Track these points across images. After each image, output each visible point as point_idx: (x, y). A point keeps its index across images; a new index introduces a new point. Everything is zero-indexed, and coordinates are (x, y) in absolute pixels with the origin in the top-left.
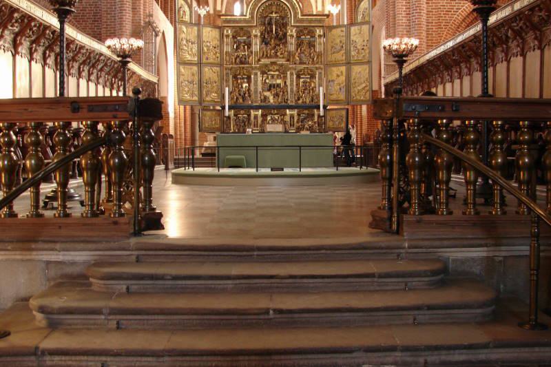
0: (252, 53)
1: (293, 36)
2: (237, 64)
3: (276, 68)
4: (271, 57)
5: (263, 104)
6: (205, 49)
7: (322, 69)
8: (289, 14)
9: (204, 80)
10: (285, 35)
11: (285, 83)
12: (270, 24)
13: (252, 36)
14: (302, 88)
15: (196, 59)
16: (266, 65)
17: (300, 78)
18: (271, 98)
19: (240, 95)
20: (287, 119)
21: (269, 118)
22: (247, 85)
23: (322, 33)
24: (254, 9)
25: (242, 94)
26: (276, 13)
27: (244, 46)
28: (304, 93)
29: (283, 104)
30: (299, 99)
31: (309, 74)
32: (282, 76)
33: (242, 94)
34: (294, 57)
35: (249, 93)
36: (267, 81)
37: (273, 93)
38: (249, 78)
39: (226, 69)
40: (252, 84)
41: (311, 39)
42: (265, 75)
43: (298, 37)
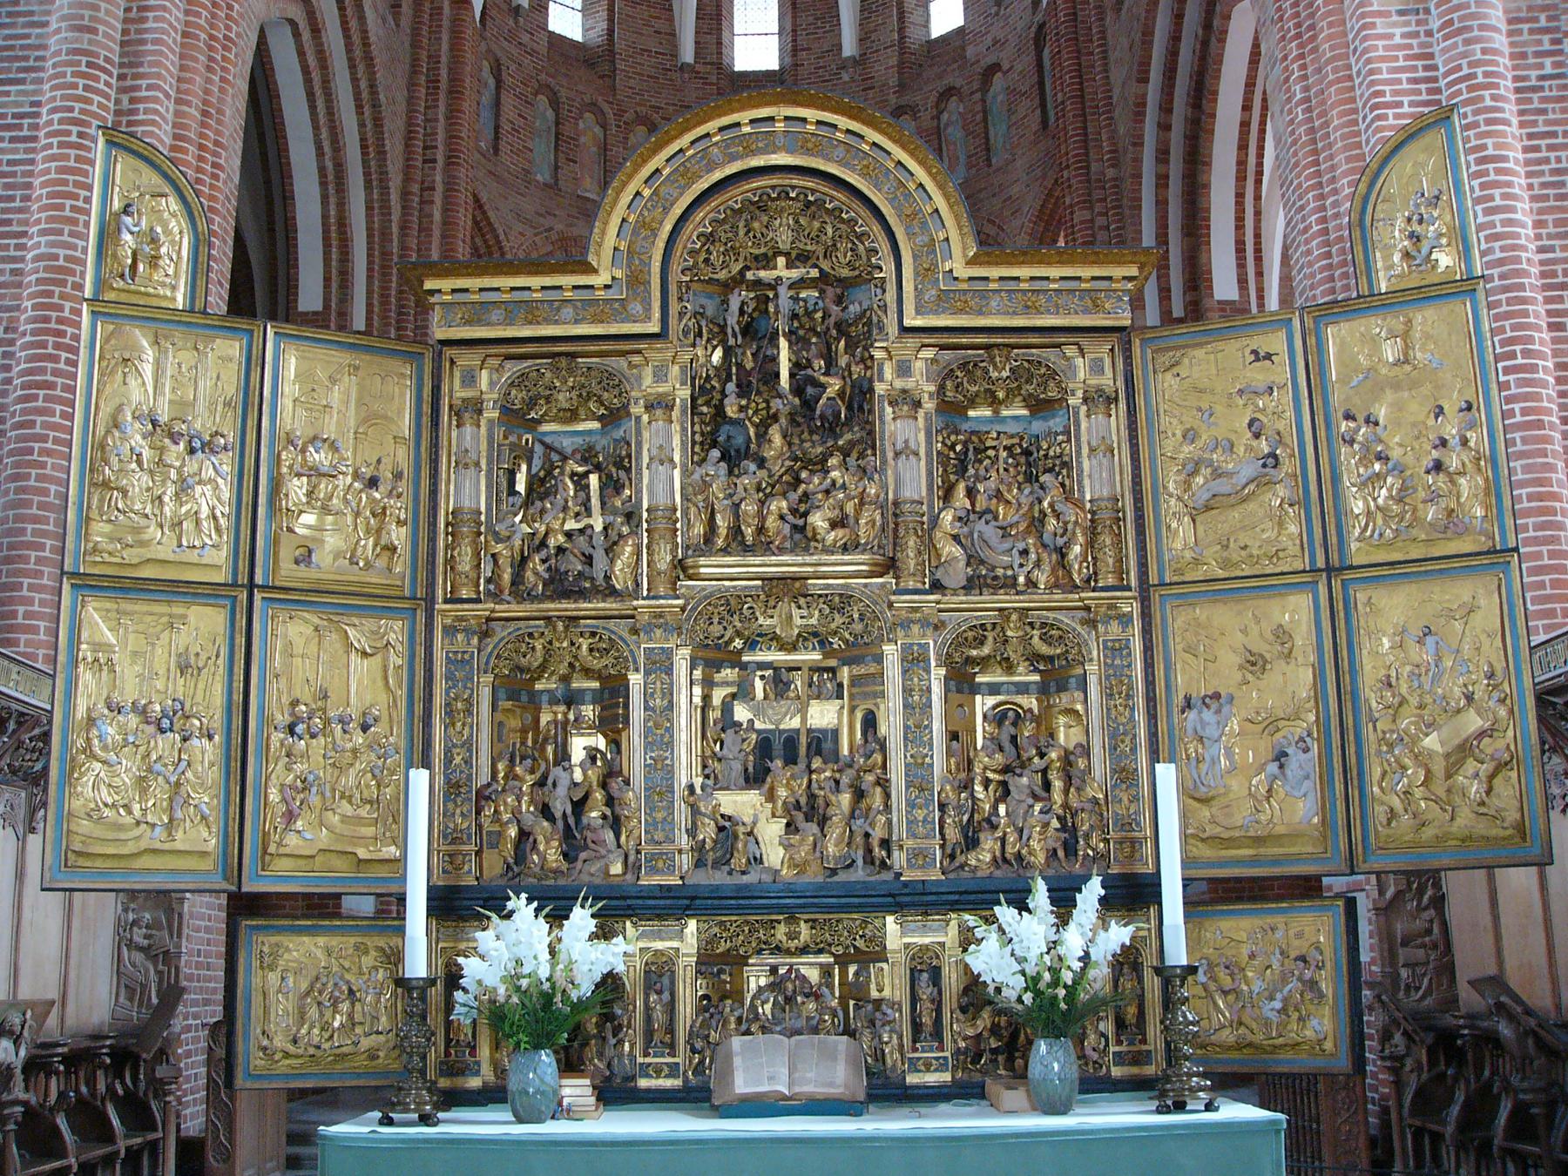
0: (629, 516)
1: (917, 404)
2: (531, 597)
3: (801, 618)
4: (763, 544)
5: (705, 878)
6: (297, 489)
7: (1125, 620)
8: (884, 247)
9: (272, 701)
10: (860, 397)
11: (870, 722)
12: (755, 330)
13: (637, 410)
14: (987, 762)
15: (221, 556)
16: (731, 605)
17: (975, 689)
18: (771, 831)
19: (546, 812)
20: (889, 983)
21: (756, 979)
22: (601, 743)
23: (1108, 380)
24: (646, 228)
25: (560, 805)
26: (798, 258)
27: (580, 481)
28: (1005, 792)
29: (859, 874)
30: (972, 843)
31: (1034, 658)
32: (845, 674)
33: (560, 805)
34: (928, 544)
35: (610, 801)
36: (741, 713)
37: (782, 793)
38: (613, 695)
39: (449, 631)
40: (635, 736)
41: (1038, 427)
42: (728, 673)
43: (951, 409)
